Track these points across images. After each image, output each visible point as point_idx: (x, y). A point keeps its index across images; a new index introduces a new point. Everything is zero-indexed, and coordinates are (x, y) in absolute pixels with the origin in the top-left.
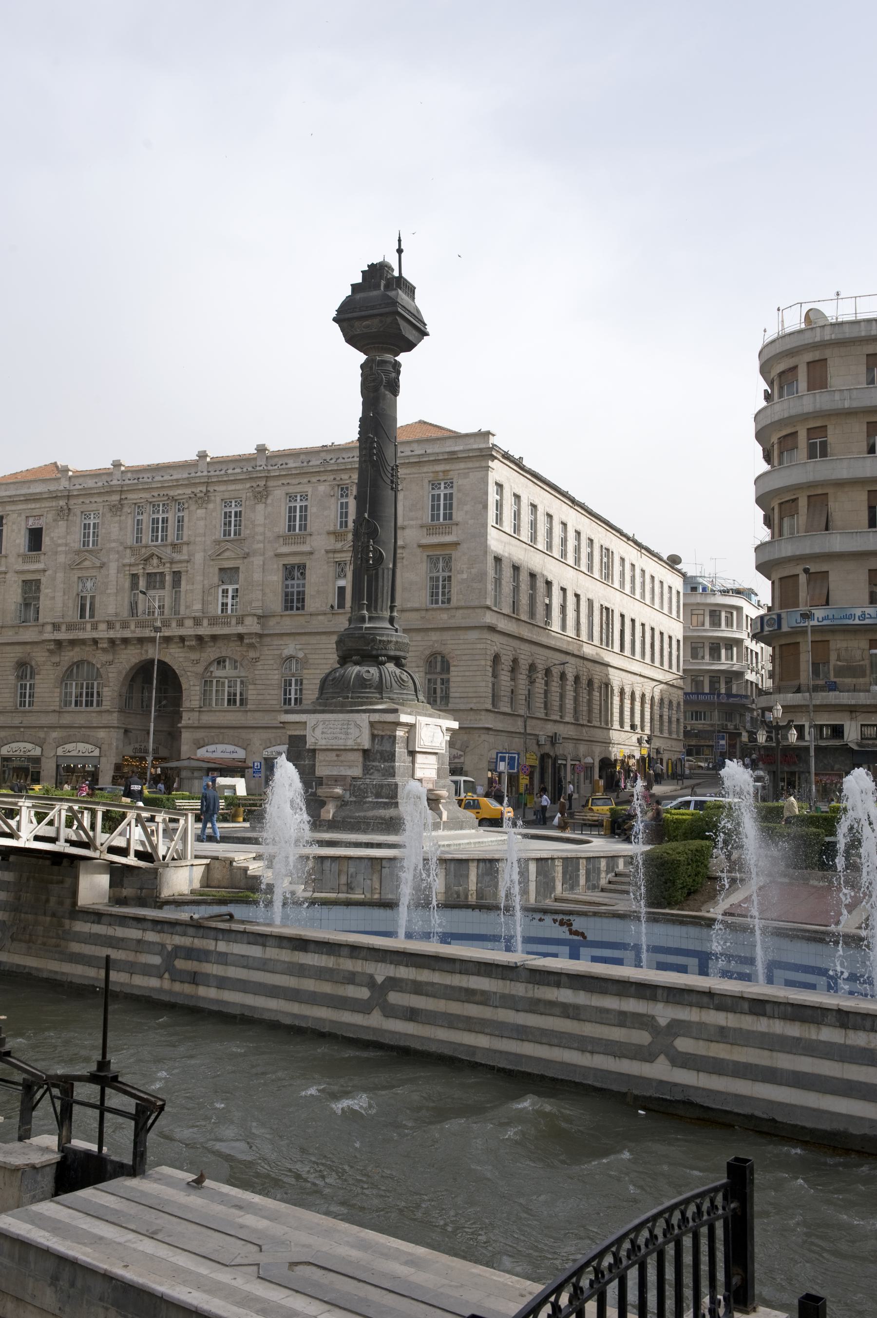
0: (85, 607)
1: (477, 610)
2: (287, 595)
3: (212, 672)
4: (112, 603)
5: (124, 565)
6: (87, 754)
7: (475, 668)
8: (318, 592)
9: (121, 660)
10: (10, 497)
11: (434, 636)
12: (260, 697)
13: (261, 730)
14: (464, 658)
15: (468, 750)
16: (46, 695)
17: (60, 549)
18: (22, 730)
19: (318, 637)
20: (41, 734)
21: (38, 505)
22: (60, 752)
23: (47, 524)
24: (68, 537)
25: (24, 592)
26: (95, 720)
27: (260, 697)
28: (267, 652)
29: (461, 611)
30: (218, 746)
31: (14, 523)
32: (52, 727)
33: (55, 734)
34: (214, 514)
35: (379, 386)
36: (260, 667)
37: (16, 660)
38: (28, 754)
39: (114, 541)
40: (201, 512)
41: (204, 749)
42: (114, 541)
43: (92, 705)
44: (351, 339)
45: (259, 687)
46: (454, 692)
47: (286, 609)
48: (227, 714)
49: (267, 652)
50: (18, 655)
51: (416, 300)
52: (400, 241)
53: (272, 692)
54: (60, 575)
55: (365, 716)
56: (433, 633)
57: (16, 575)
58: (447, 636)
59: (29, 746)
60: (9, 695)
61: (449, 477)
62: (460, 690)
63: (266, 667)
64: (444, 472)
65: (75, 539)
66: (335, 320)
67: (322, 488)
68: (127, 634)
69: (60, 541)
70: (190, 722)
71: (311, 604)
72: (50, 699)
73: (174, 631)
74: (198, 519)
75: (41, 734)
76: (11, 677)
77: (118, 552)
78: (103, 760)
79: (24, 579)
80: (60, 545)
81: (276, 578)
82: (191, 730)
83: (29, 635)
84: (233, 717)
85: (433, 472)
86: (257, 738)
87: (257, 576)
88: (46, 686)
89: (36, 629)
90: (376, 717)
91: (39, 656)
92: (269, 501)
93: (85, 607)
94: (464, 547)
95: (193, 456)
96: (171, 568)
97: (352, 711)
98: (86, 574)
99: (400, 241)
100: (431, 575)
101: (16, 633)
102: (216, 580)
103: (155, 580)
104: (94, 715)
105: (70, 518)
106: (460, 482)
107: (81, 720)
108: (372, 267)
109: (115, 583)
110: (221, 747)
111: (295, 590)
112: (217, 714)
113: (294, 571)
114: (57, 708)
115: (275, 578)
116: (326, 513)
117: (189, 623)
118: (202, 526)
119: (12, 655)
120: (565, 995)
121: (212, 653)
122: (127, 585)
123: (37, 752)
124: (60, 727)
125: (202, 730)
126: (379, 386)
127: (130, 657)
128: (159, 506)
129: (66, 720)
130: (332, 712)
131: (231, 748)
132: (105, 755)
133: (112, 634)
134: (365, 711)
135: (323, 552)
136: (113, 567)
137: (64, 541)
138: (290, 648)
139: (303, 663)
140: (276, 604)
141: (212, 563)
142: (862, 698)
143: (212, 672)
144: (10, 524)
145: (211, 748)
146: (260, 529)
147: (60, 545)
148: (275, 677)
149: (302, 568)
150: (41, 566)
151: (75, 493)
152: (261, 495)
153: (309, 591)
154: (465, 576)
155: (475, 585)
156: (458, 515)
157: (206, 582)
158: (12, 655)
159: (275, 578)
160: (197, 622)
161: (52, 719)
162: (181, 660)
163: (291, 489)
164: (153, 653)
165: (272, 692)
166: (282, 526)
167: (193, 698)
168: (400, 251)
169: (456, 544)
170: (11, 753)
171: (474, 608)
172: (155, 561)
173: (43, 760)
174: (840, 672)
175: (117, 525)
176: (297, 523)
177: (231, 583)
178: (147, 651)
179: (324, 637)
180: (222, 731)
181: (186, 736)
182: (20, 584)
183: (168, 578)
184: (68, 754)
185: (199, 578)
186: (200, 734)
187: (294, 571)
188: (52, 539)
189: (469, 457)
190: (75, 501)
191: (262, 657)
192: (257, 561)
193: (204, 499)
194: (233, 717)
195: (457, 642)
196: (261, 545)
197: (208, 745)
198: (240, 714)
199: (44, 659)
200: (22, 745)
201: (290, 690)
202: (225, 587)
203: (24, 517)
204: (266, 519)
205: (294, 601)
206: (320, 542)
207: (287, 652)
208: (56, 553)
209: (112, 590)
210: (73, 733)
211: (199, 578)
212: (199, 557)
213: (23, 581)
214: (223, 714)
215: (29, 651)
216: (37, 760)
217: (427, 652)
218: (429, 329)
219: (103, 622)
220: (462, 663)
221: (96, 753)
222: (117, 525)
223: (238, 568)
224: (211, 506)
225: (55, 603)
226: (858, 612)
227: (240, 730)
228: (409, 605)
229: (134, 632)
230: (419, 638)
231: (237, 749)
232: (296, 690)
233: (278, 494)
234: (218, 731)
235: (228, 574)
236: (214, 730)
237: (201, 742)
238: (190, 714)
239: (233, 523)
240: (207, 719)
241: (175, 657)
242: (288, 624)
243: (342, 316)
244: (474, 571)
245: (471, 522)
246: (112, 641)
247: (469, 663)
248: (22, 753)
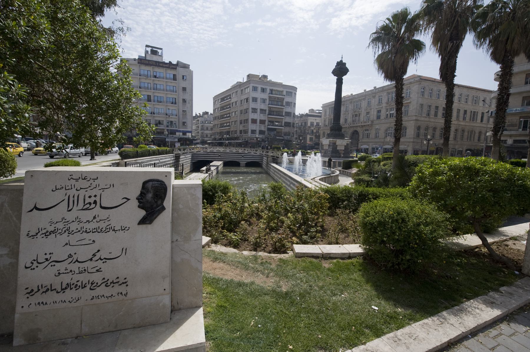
4: (350, 120)
46: (407, 134)
71: (382, 118)
73: (358, 125)
84: (367, 140)
86: (371, 144)
87: (372, 113)
103: (356, 115)
113: (379, 111)
118: (364, 104)
120: (282, 174)
121: (364, 128)
127: (351, 130)
138: (377, 127)
139: (379, 129)
140: (375, 118)
142: (513, 133)
148: (374, 132)
149: (380, 111)
152: (374, 97)
156: (411, 96)
160: (362, 123)
164: (355, 129)
166: (377, 103)
169: (410, 103)
174: (509, 126)
181: (359, 144)
187: (379, 111)
192: (373, 110)
193: (364, 99)
194: (367, 140)
204: (374, 102)
205: (378, 117)
206: (384, 105)
212: (363, 111)
226: (515, 109)
233: (377, 96)
235: (368, 113)
239: (369, 103)
240: (364, 141)
241: (359, 129)
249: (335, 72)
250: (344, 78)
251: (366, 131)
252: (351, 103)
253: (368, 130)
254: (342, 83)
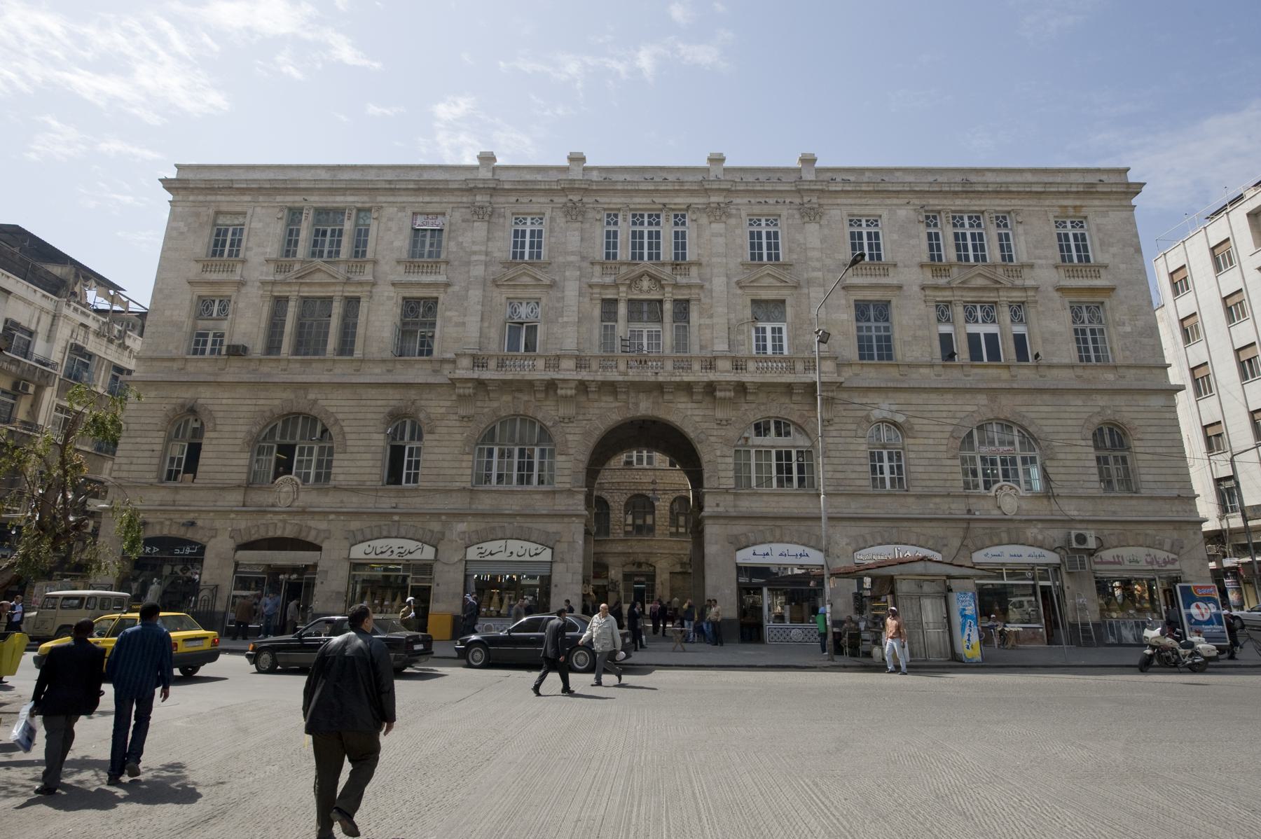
0: (522, 334)
1: (1154, 371)
2: (860, 339)
3: (747, 439)
5: (590, 286)
6: (527, 558)
7: (1170, 443)
8: (915, 337)
9: (589, 417)
10: (390, 182)
11: (1102, 401)
12: (838, 475)
13: (847, 523)
14: (1149, 429)
15: (1182, 552)
16: (446, 464)
17: (475, 258)
18: (396, 518)
19: (925, 396)
20: (436, 526)
21: (436, 199)
22: (473, 553)
23: (451, 224)
24: (490, 244)
25: (405, 314)
26: (541, 505)
27: (838, 475)
28: (844, 414)
29: (1133, 371)
30: (774, 546)
31: (390, 219)
32: (459, 516)
33: (461, 527)
34: (738, 231)
36: (835, 434)
37: (388, 410)
38: (409, 557)
39: (573, 253)
40: (718, 227)
41: (750, 550)
42: (573, 253)
43: (529, 482)
45: (836, 461)
47: (862, 357)
48: (782, 498)
49: (844, 414)
50: (392, 403)
53: (859, 468)
54: (475, 294)
56: (1099, 397)
57: (392, 288)
58: (1120, 401)
59: (411, 545)
60: (371, 463)
61: (1082, 214)
62: (1153, 471)
63: (843, 433)
64: (1075, 207)
65: (502, 247)
67: (902, 213)
68: (613, 376)
69: (475, 248)
70: (721, 509)
72: (454, 472)
74: (713, 235)
75: (436, 526)
76: (376, 436)
77: (580, 268)
78: (558, 568)
79: (407, 295)
80: (475, 253)
81: (843, 318)
82: (722, 521)
83: (417, 373)
84: (791, 503)
85: (1060, 207)
88: (445, 454)
89: (428, 366)
91: (434, 407)
92: (823, 222)
93: (522, 334)
94: (1121, 293)
98: (520, 293)
100: (1076, 326)
101: (388, 371)
102: (748, 313)
104: (537, 497)
105: (493, 220)
106: (1099, 221)
107: (512, 504)
109: (575, 309)
110: (778, 548)
111: (874, 333)
112: (765, 498)
113: (872, 311)
114: (469, 485)
115: (845, 317)
116: (913, 242)
117: (724, 365)
119: (379, 403)
121: (753, 412)
122: (597, 312)
123: (428, 553)
124: (475, 515)
125: (743, 522)
128: (642, 216)
129: (485, 503)
131: (798, 549)
132: (562, 560)
133: (584, 375)
135: (916, 288)
136: (571, 290)
137: (483, 248)
138: (883, 408)
141: (739, 292)
143: (747, 439)
144: (384, 220)
145: (760, 549)
146: (816, 254)
147: (475, 253)
149: (883, 310)
150: (441, 278)
151: (506, 187)
153: (897, 335)
154: (1128, 329)
155: (1145, 341)
157: (732, 316)
158: (379, 403)
159: (845, 317)
161: (457, 503)
162: (697, 419)
163: (856, 211)
165: (859, 468)
167: (722, 474)
170: (373, 556)
171: (1150, 367)
172: (646, 283)
173: (438, 568)
175: (577, 233)
176: (865, 253)
177: (768, 320)
178: (637, 405)
179: (933, 396)
180: (779, 523)
181: (712, 531)
182: (400, 301)
183: (668, 306)
184: (490, 558)
185: (721, 309)
186: (739, 528)
187: (872, 311)
188: (460, 244)
189: (1111, 192)
190: (502, 199)
191: (836, 420)
192: (816, 294)
193: (719, 212)
194: (791, 503)
195: (1136, 409)
196: (819, 274)
197: (754, 544)
198: (806, 498)
199: (443, 410)
200: (395, 543)
202: (760, 325)
203: (409, 213)
205: (877, 348)
207: (876, 414)
208: (468, 263)
209: (571, 316)
210: (495, 525)
211: (721, 309)
212: (719, 284)
213: (404, 298)
214: (776, 498)
215: (414, 397)
216: (425, 568)
217: (1097, 420)
219: (570, 357)
220: (1148, 436)
221: (546, 555)
222: (577, 233)
223: (783, 302)
224: (733, 221)
225: (464, 326)
227: (810, 523)
228: (1055, 360)
229: (626, 374)
230: (1080, 403)
231: (808, 550)
232: (891, 467)
234: (771, 523)
236: (764, 523)
237: (743, 539)
238: (719, 499)
239: (763, 249)
240: (748, 505)
241: (686, 415)
242: (871, 375)
244: (1140, 323)
245: (1123, 266)
246: (583, 386)
247: (1158, 436)
248: (395, 556)
251: (761, 429)
252: (574, 212)
253: (782, 427)
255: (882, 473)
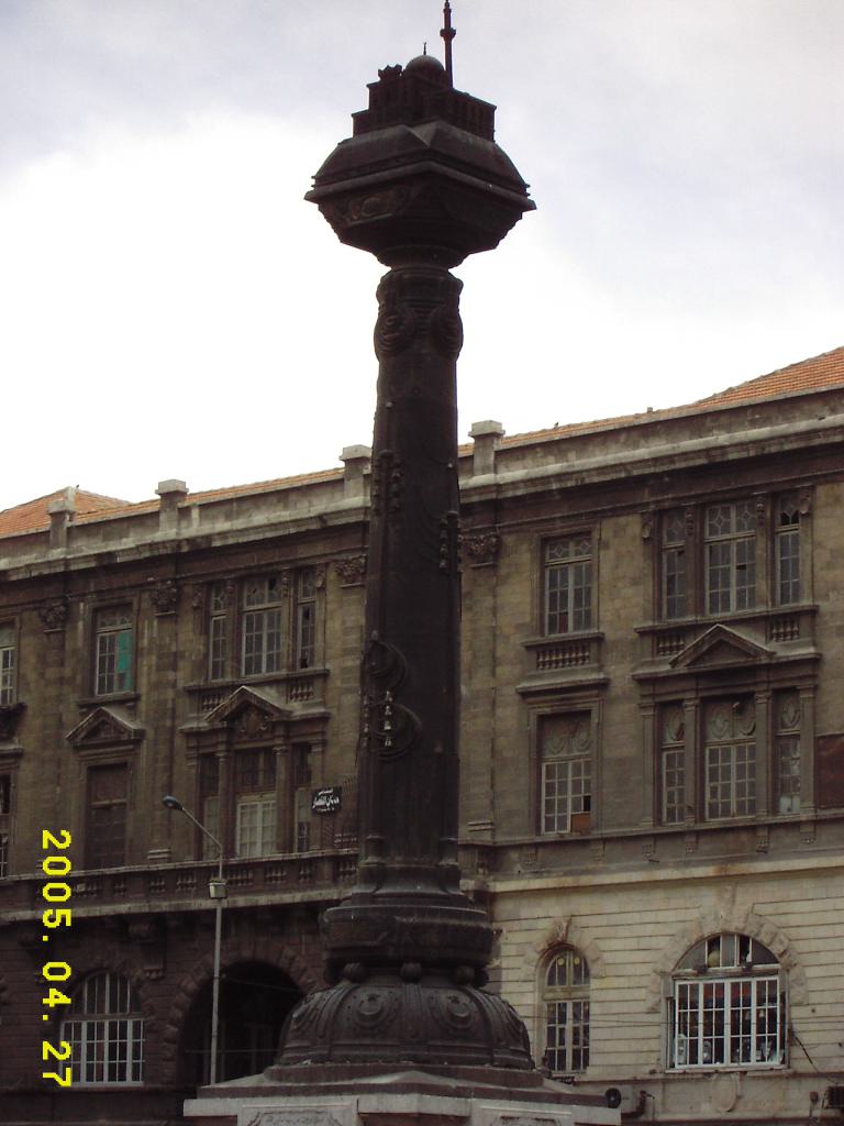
35: (418, 339)
44: (350, 235)
51: (496, 137)
52: (447, 12)
55: (348, 1101)
66: (310, 197)
90: (372, 1103)
95: (551, 426)
96: (287, 737)
97: (327, 1091)
99: (447, 12)
108: (389, 75)
126: (418, 339)
130: (289, 1092)
134: (351, 1090)
168: (448, 34)
201: (562, 1031)
218: (533, 194)
243: (331, 188)
249: (352, 195)
250: (472, 270)
254: (448, 337)
255: (562, 1042)
